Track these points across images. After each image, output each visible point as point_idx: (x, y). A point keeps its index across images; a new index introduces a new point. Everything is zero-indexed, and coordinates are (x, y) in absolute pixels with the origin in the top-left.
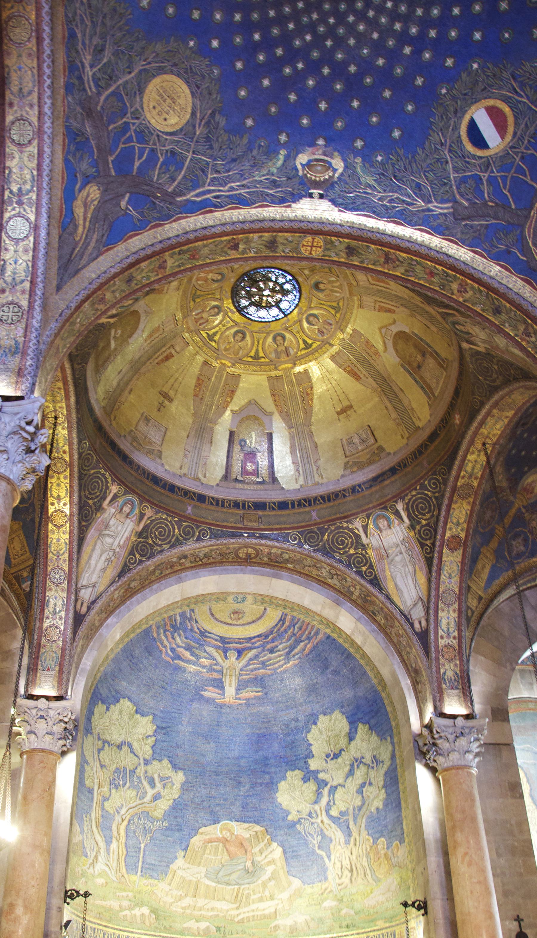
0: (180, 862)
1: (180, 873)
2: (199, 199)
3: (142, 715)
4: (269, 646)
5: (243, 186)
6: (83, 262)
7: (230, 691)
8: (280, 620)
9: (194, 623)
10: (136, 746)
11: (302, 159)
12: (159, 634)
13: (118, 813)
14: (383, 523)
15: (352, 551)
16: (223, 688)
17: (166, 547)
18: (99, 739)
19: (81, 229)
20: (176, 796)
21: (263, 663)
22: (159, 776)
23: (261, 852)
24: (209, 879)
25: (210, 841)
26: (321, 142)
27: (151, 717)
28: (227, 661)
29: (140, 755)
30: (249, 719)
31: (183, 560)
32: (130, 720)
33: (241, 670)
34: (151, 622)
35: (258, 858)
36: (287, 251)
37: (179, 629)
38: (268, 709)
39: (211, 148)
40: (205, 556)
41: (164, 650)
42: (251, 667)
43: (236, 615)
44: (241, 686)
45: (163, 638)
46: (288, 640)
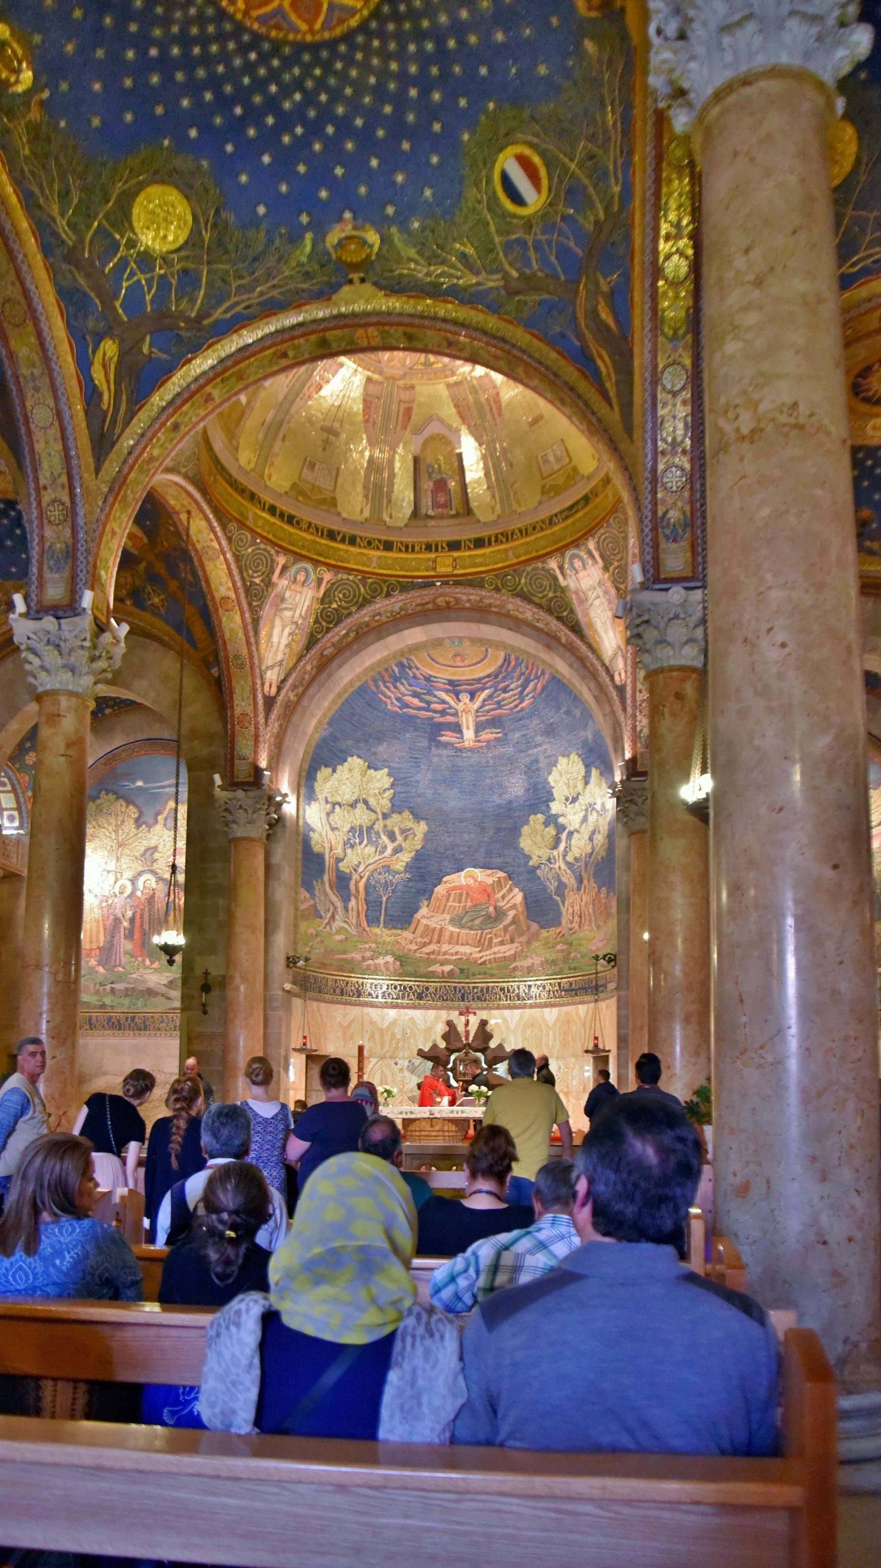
0: (424, 911)
1: (424, 921)
2: (229, 315)
3: (376, 769)
4: (501, 685)
5: (274, 286)
6: (117, 431)
7: (469, 734)
8: (505, 660)
9: (414, 670)
10: (372, 801)
11: (333, 238)
12: (377, 687)
13: (355, 870)
14: (577, 564)
15: (551, 595)
16: (460, 731)
17: (354, 609)
18: (327, 802)
19: (106, 397)
20: (419, 847)
21: (498, 703)
22: (400, 828)
23: (503, 897)
24: (454, 925)
25: (454, 889)
26: (348, 215)
27: (386, 770)
28: (461, 704)
29: (378, 810)
30: (491, 762)
31: (377, 618)
32: (364, 775)
33: (477, 711)
34: (364, 679)
35: (501, 904)
36: (343, 345)
37: (400, 678)
38: (509, 750)
39: (226, 252)
40: (401, 609)
41: (389, 701)
42: (487, 708)
43: (458, 658)
44: (479, 728)
45: (385, 689)
46: (518, 680)
